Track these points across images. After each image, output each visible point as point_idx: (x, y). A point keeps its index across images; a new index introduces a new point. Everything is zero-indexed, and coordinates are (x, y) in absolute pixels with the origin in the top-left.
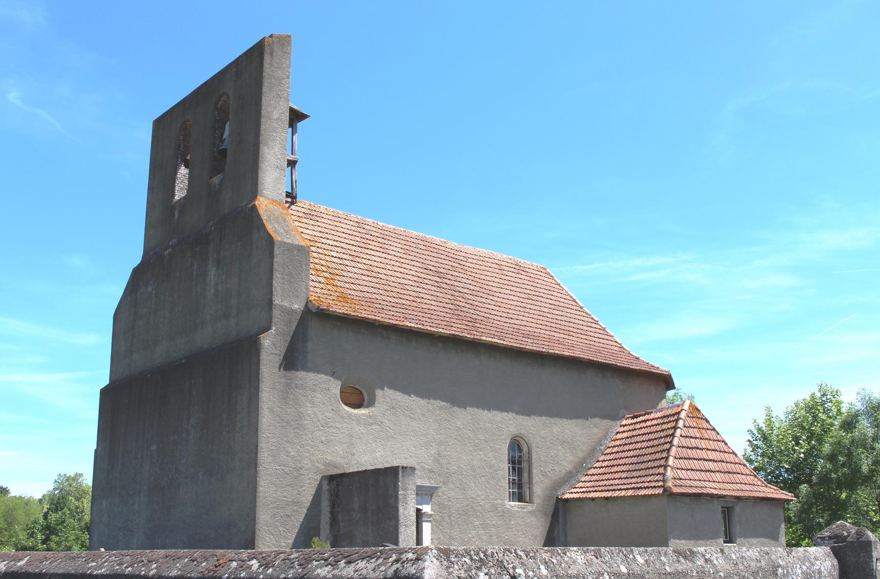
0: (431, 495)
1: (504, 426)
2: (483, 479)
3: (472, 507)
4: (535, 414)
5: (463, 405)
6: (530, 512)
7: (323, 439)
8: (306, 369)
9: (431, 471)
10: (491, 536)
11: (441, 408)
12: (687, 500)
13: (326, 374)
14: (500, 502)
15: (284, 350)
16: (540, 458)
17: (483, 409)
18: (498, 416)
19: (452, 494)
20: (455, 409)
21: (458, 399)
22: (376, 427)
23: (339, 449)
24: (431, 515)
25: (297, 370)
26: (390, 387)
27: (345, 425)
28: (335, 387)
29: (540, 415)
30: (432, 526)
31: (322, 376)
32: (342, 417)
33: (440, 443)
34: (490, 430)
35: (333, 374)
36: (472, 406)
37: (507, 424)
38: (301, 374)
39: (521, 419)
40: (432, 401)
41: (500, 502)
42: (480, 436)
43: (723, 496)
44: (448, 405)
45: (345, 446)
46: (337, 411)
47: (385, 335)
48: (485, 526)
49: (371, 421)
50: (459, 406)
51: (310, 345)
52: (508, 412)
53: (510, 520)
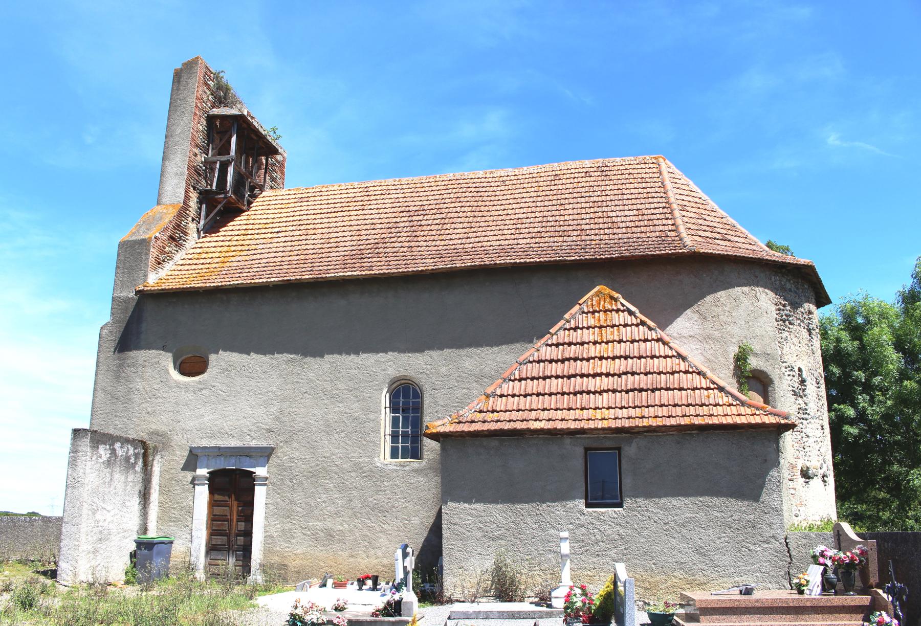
0: (269, 457)
1: (378, 370)
2: (342, 434)
3: (323, 467)
4: (431, 348)
5: (319, 353)
6: (416, 471)
7: (149, 409)
8: (138, 348)
9: (270, 431)
10: (351, 500)
11: (288, 362)
12: (494, 443)
13: (157, 349)
14: (366, 459)
15: (119, 335)
16: (436, 403)
17: (348, 353)
18: (368, 360)
19: (297, 454)
20: (309, 359)
21: (312, 347)
22: (207, 392)
23: (164, 418)
24: (266, 478)
25: (131, 350)
26: (225, 350)
27: (173, 394)
28: (167, 360)
29: (441, 348)
30: (268, 490)
31: (154, 352)
32: (170, 387)
33: (284, 400)
34: (362, 380)
35: (164, 348)
36: (331, 352)
37: (390, 365)
38: (133, 353)
39: (405, 357)
40: (276, 356)
41: (366, 459)
42: (342, 386)
43: (582, 431)
44: (298, 357)
45: (171, 414)
46: (165, 379)
47: (225, 298)
48: (341, 488)
49: (201, 386)
50: (314, 355)
51: (144, 326)
52: (385, 351)
53: (382, 481)
